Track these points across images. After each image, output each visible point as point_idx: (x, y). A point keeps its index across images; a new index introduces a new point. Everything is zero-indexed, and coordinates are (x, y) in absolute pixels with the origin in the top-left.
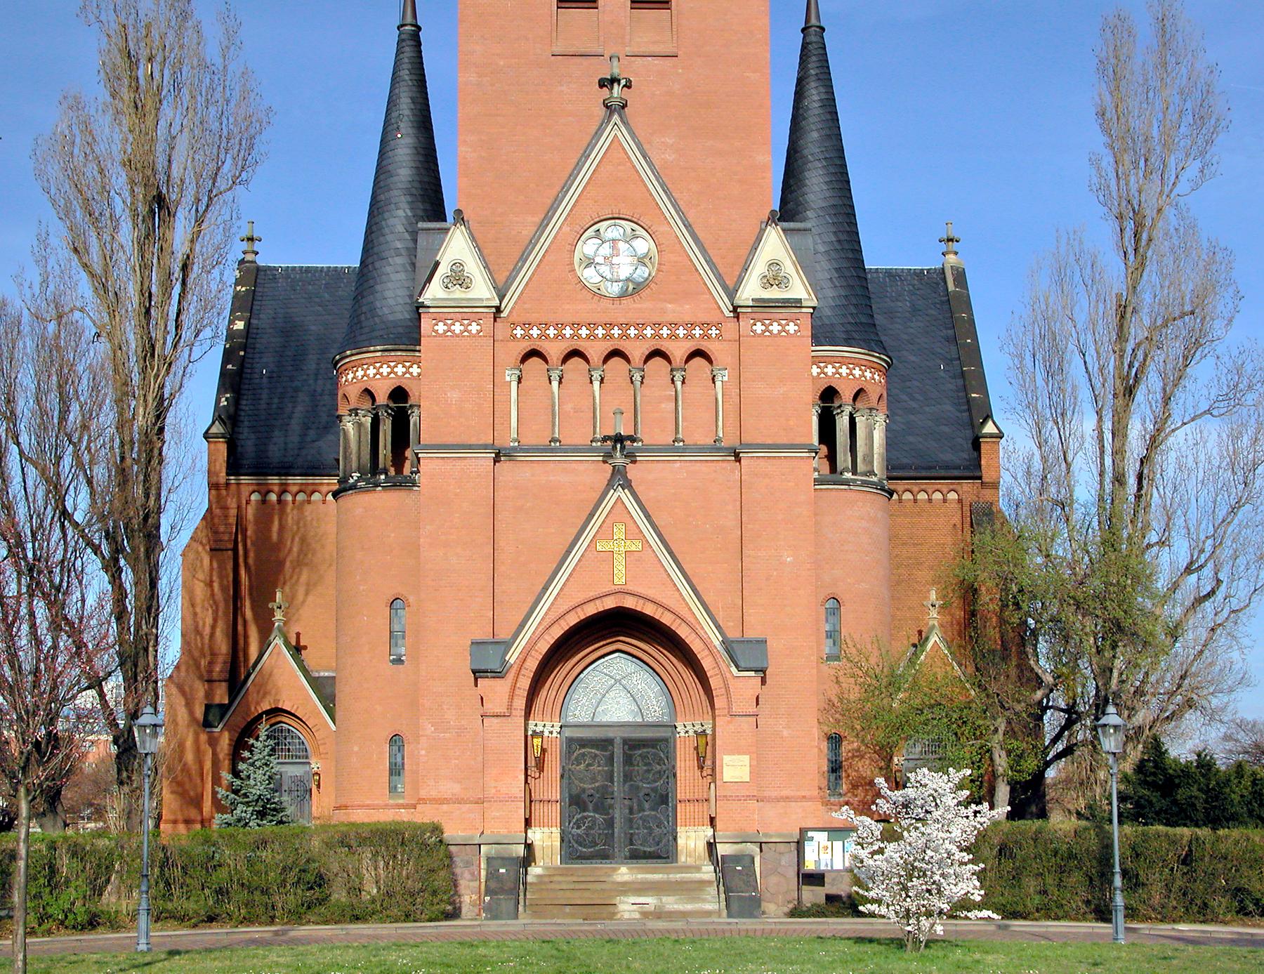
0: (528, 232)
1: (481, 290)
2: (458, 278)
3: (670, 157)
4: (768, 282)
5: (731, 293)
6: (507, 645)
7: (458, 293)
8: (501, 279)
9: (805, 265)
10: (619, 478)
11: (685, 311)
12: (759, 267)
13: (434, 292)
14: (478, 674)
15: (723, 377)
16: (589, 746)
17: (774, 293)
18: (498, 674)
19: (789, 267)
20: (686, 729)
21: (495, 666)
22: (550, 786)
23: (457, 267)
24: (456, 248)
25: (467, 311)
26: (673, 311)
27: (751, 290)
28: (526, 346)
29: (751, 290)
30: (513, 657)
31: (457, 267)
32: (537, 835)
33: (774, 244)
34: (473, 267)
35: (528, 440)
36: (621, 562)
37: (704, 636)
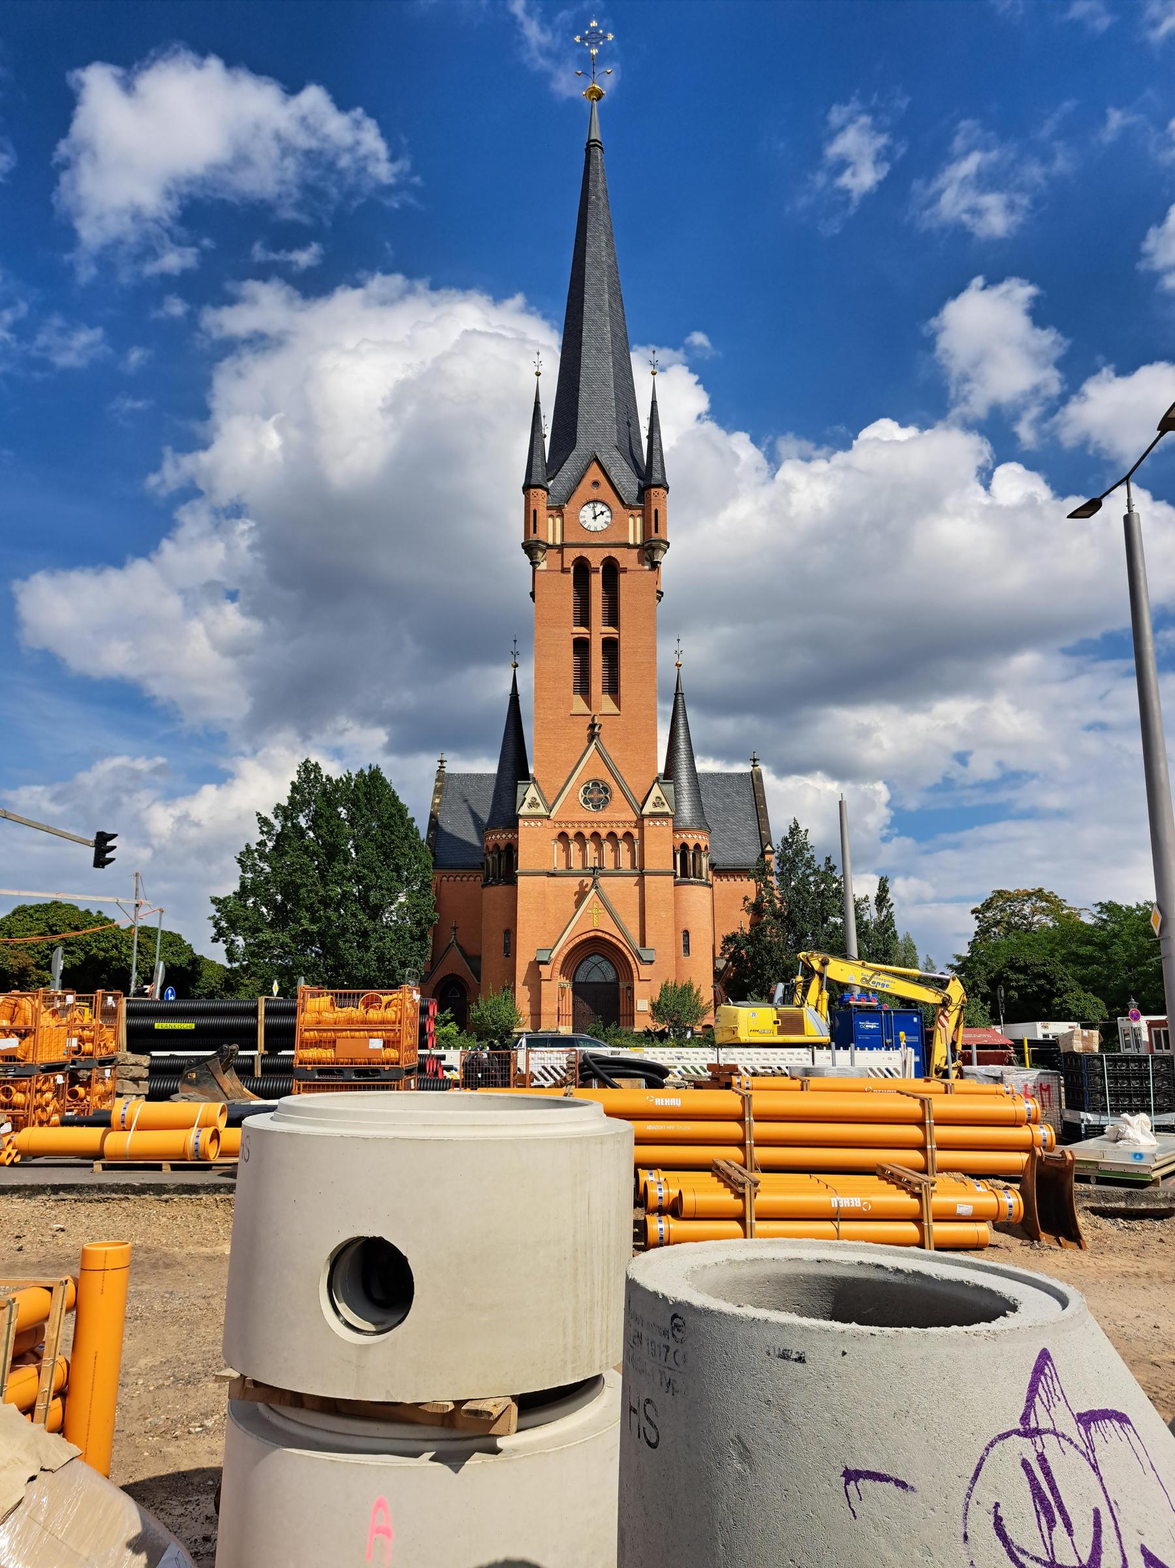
0: (562, 784)
3: (617, 754)
4: (655, 805)
6: (552, 950)
8: (551, 802)
12: (652, 799)
13: (524, 810)
17: (658, 810)
18: (546, 963)
21: (546, 959)
24: (532, 792)
29: (647, 810)
30: (553, 956)
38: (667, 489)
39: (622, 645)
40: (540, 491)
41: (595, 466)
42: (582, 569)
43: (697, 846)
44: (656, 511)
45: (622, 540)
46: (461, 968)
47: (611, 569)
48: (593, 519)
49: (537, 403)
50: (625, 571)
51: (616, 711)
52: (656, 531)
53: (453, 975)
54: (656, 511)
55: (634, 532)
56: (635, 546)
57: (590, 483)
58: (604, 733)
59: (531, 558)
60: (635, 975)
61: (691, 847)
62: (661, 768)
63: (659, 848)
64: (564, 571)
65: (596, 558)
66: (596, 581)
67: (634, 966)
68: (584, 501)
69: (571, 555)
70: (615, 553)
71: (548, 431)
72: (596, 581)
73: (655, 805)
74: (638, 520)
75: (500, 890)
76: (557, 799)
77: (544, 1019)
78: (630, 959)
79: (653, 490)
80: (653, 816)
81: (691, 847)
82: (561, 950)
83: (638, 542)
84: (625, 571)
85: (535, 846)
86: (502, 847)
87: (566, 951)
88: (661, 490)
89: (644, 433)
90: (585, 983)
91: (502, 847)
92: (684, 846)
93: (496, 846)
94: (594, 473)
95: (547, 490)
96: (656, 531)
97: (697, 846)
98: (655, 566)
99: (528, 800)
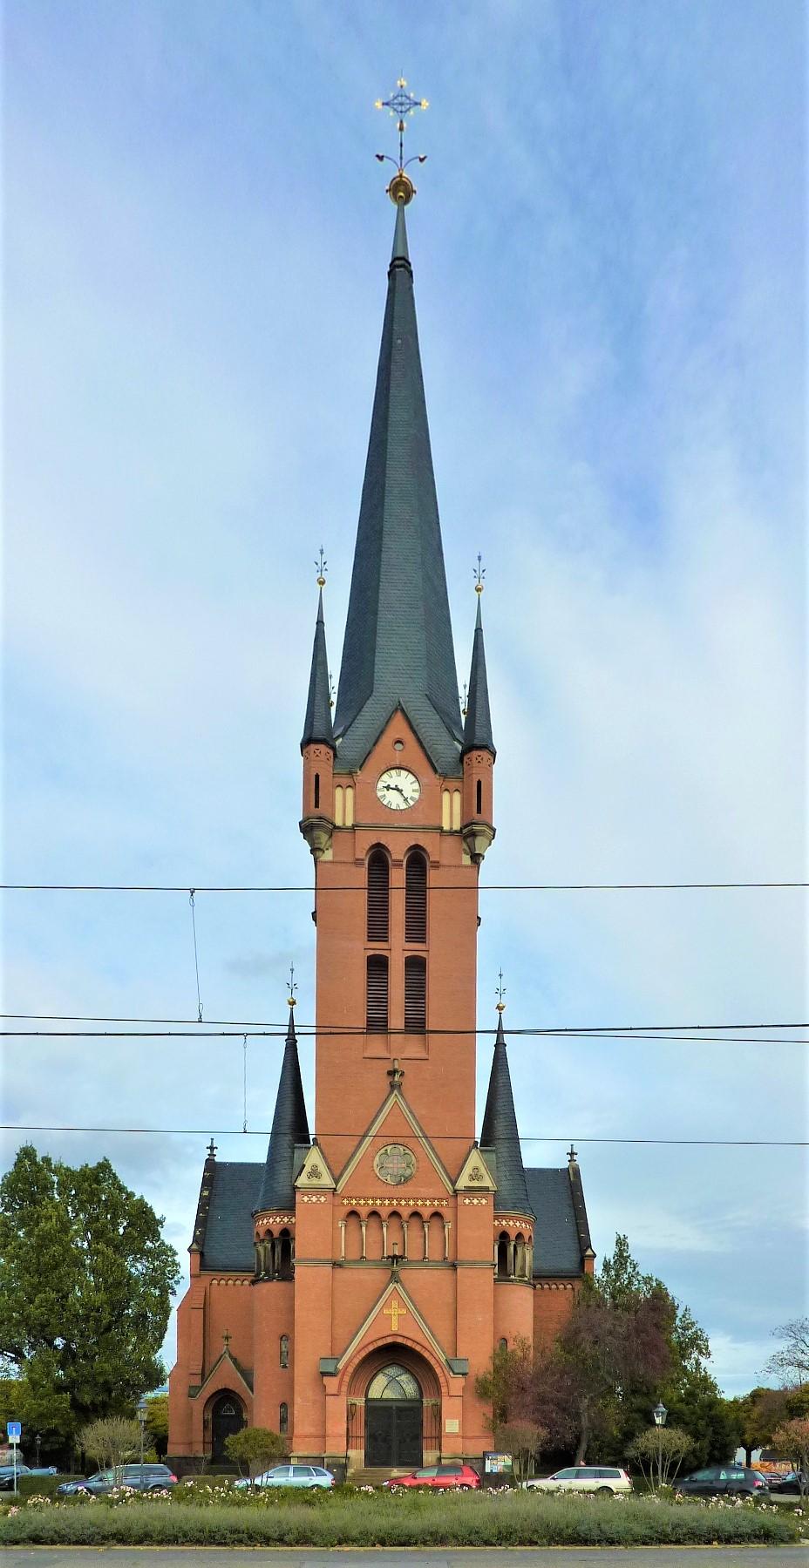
1: (327, 1180)
2: (315, 1173)
4: (472, 1178)
5: (454, 1183)
6: (338, 1360)
7: (315, 1181)
8: (337, 1173)
9: (489, 1168)
10: (394, 1278)
11: (431, 1192)
12: (467, 1170)
14: (324, 1374)
15: (449, 1226)
16: (375, 1410)
17: (476, 1184)
19: (483, 1171)
20: (427, 1402)
21: (331, 1370)
22: (360, 1430)
23: (315, 1167)
25: (319, 1190)
26: (424, 1192)
27: (463, 1182)
28: (349, 1209)
29: (463, 1182)
30: (341, 1366)
31: (315, 1167)
32: (352, 1453)
33: (475, 1159)
34: (323, 1168)
35: (350, 1257)
36: (394, 1318)
37: (437, 1355)
38: (494, 754)
39: (431, 967)
40: (322, 747)
41: (399, 714)
42: (379, 859)
43: (520, 1236)
44: (479, 783)
45: (434, 823)
46: (237, 1383)
47: (417, 860)
48: (399, 789)
49: (320, 623)
50: (436, 865)
51: (424, 1056)
52: (479, 811)
53: (225, 1390)
54: (479, 783)
55: (451, 812)
56: (452, 833)
57: (391, 741)
58: (407, 1083)
59: (312, 843)
60: (444, 1390)
61: (513, 1237)
62: (478, 1134)
63: (478, 1242)
64: (358, 862)
65: (398, 850)
66: (398, 877)
67: (442, 1380)
68: (384, 768)
69: (366, 840)
70: (424, 840)
71: (334, 682)
72: (398, 877)
73: (472, 1178)
74: (457, 797)
75: (271, 1290)
76: (345, 1168)
77: (329, 1441)
78: (438, 1370)
79: (475, 753)
80: (469, 1189)
81: (513, 1237)
82: (350, 1360)
83: (457, 826)
84: (436, 865)
85: (315, 1229)
86: (276, 1234)
87: (356, 1361)
88: (485, 754)
89: (463, 693)
90: (381, 1400)
91: (276, 1234)
92: (504, 1236)
93: (269, 1232)
94: (398, 724)
95: (333, 748)
96: (479, 811)
97: (520, 1236)
98: (476, 858)
99: (307, 1169)
